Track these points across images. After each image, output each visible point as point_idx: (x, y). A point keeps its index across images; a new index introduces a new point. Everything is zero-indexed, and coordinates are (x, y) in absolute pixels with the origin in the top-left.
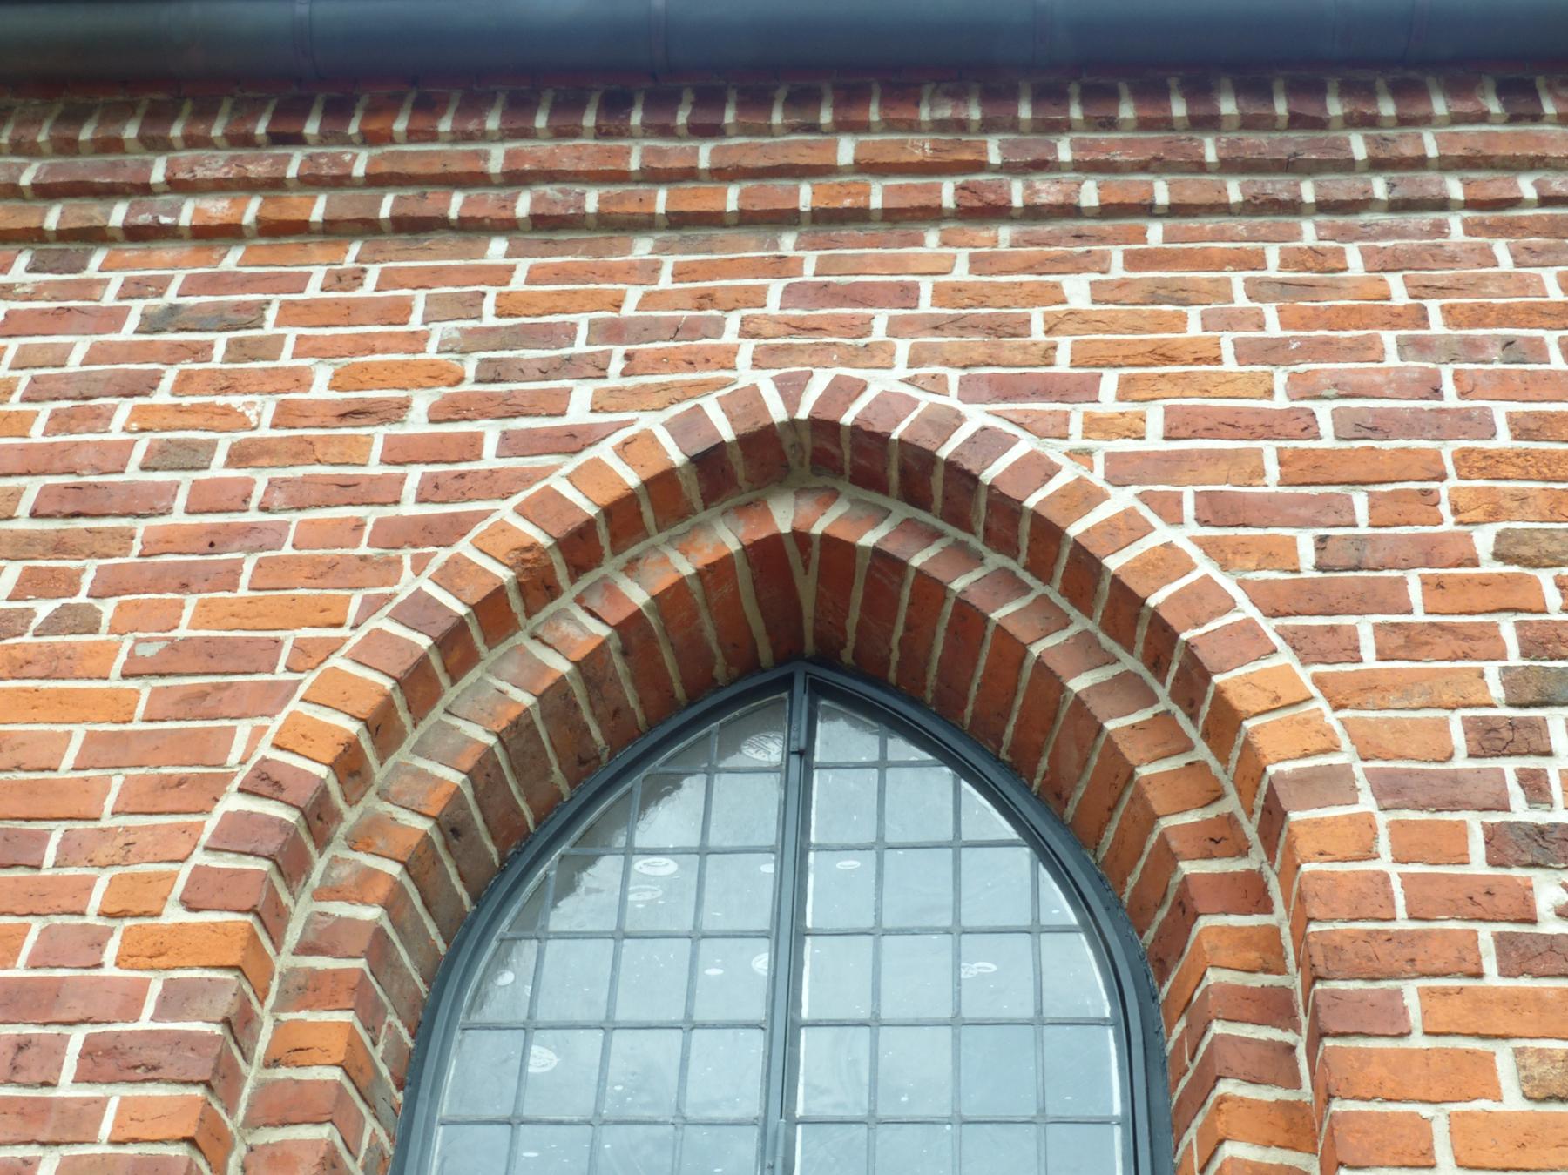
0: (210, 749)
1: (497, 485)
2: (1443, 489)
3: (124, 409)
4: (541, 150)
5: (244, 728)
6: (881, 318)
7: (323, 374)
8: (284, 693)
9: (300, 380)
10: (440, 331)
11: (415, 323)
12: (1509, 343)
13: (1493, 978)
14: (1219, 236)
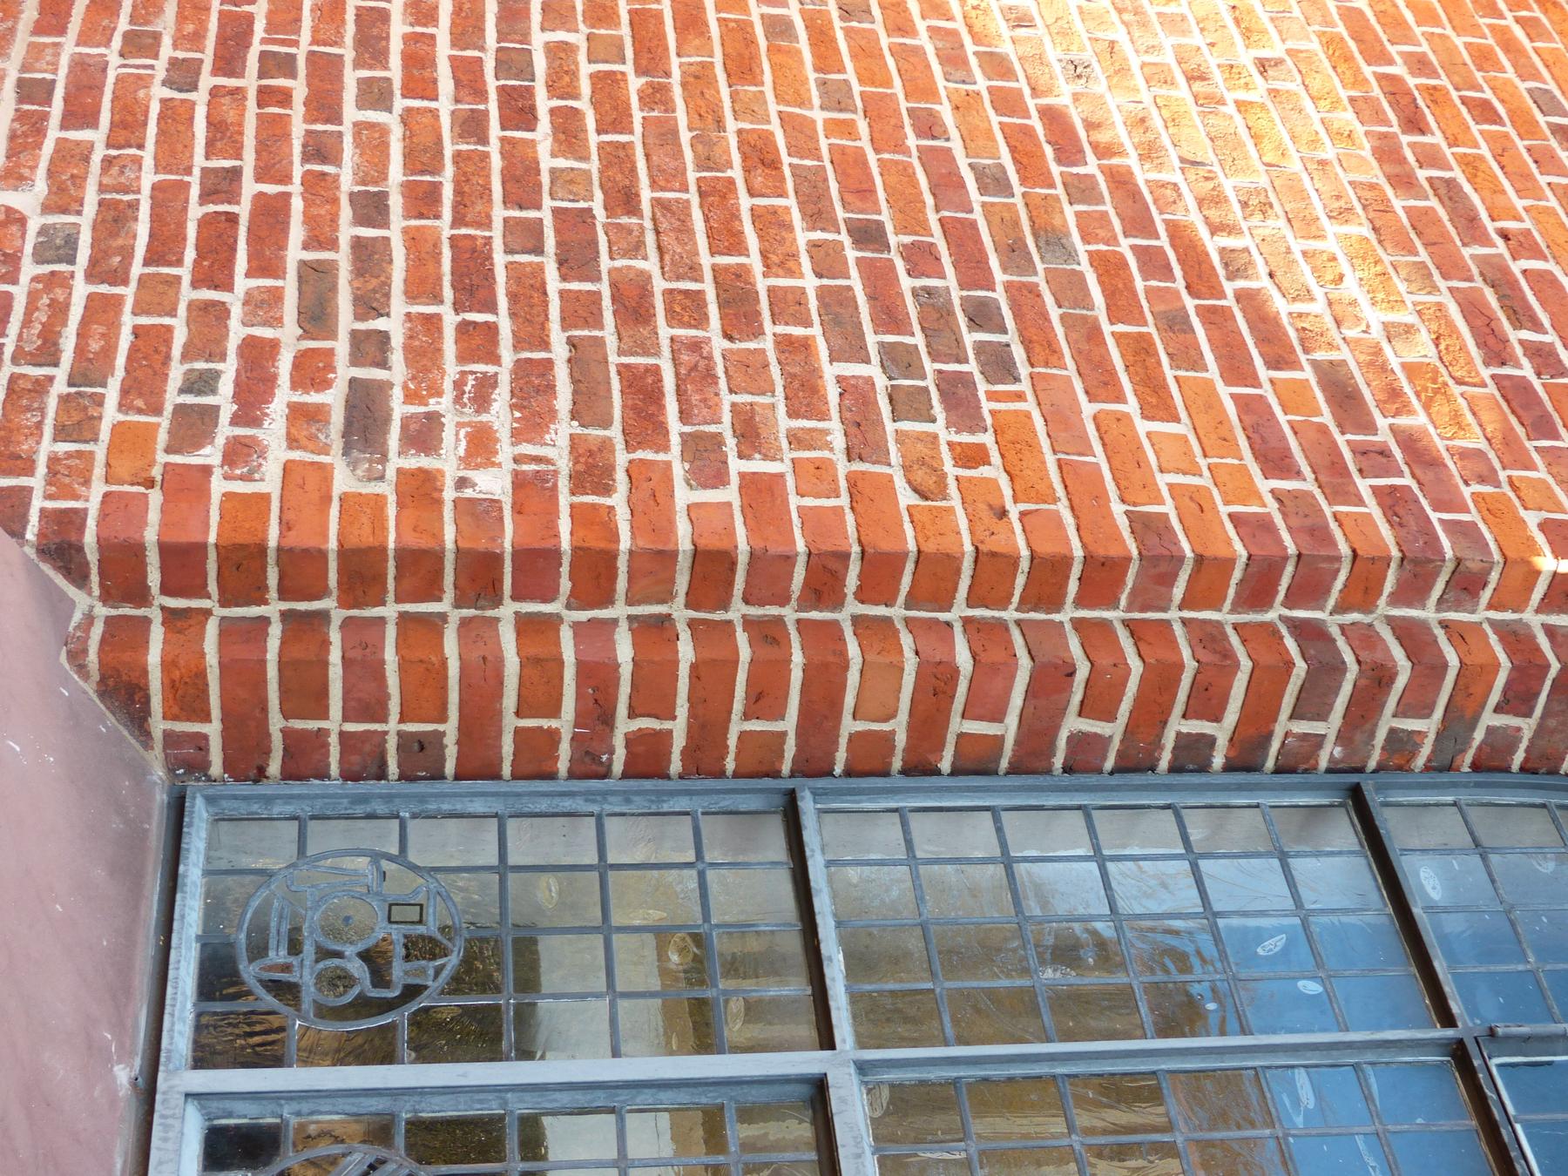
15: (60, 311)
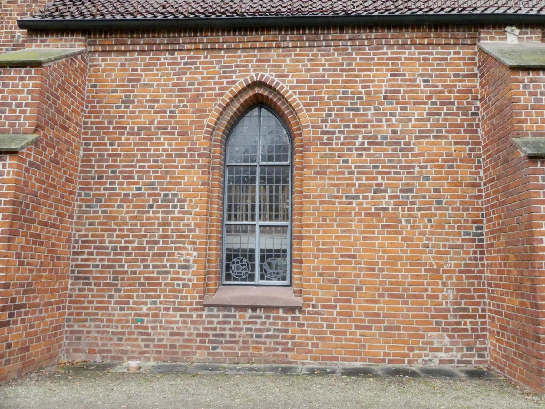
0: (202, 122)
1: (226, 88)
2: (323, 90)
3: (184, 77)
4: (227, 37)
5: (205, 120)
6: (266, 64)
7: (205, 72)
8: (208, 116)
9: (203, 73)
10: (218, 66)
11: (215, 65)
12: (334, 69)
13: (319, 146)
14: (305, 51)
15: (166, 301)
